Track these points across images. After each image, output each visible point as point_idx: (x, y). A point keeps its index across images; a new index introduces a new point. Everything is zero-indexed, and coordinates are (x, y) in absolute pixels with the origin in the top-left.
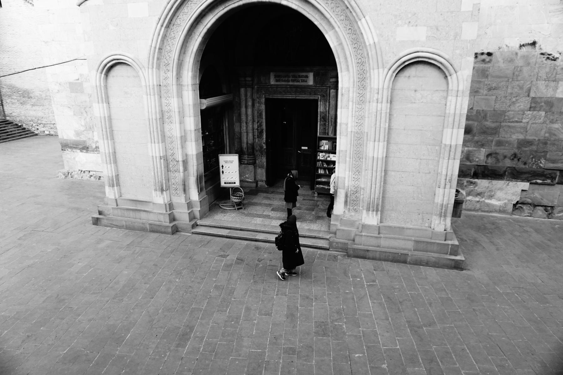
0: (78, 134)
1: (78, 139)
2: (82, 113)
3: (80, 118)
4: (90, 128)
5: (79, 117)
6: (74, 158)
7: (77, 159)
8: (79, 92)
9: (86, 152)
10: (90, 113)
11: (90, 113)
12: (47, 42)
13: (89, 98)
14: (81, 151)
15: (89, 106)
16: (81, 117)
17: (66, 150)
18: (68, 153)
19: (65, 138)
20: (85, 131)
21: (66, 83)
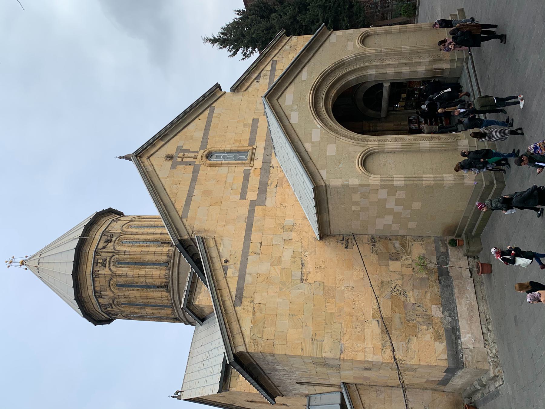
0: (437, 338)
1: (444, 338)
2: (413, 326)
3: (419, 330)
4: (429, 319)
5: (418, 331)
6: (471, 350)
7: (471, 347)
8: (391, 324)
9: (459, 330)
10: (412, 315)
11: (412, 315)
12: (341, 350)
13: (396, 313)
14: (459, 338)
15: (405, 315)
16: (417, 329)
17: (462, 360)
18: (466, 359)
19: (446, 357)
20: (434, 327)
21: (382, 337)
